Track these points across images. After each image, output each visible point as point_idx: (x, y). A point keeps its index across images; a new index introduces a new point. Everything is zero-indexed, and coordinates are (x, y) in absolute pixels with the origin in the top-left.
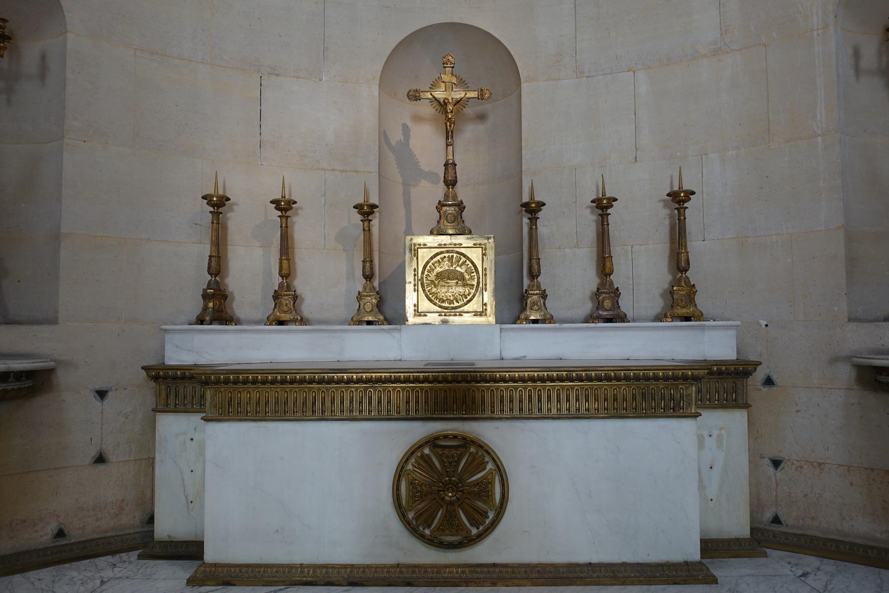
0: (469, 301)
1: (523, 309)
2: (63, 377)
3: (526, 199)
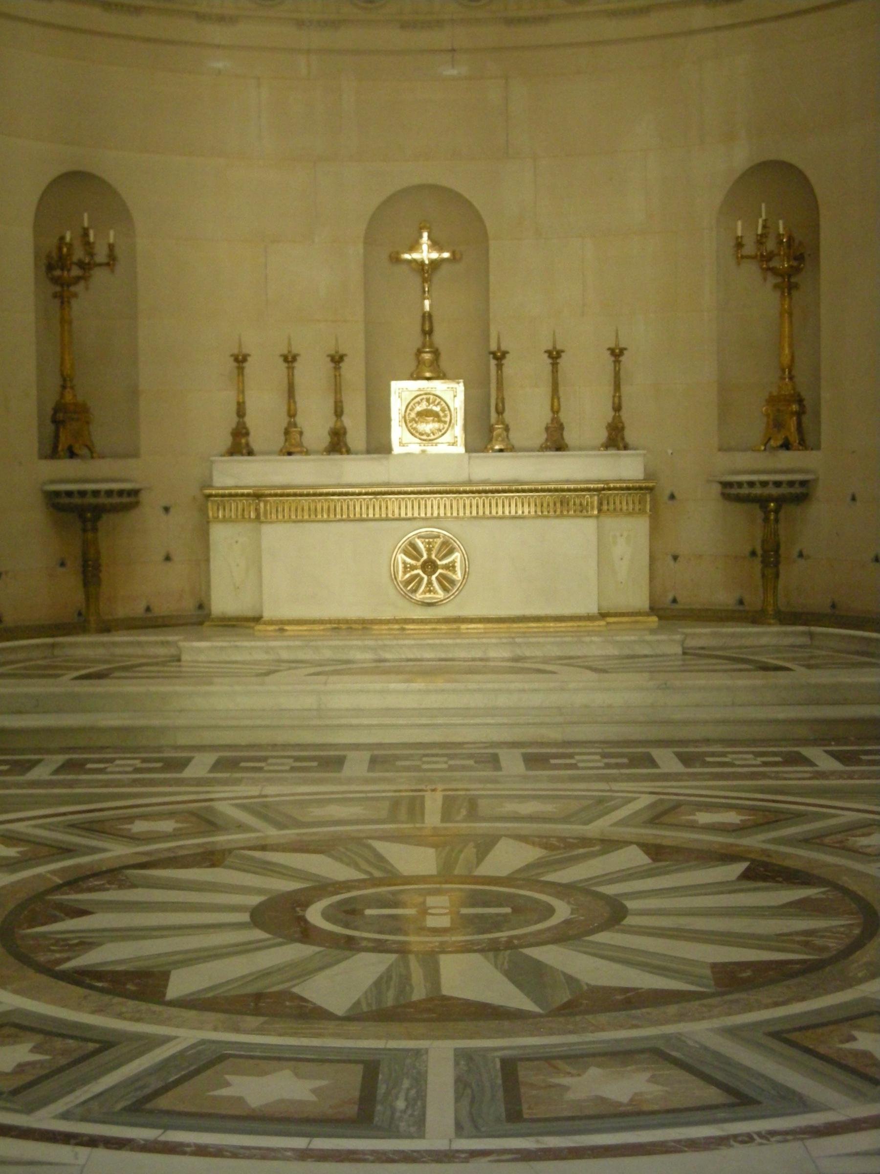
0: (443, 434)
1: (490, 440)
2: (144, 497)
3: (493, 347)
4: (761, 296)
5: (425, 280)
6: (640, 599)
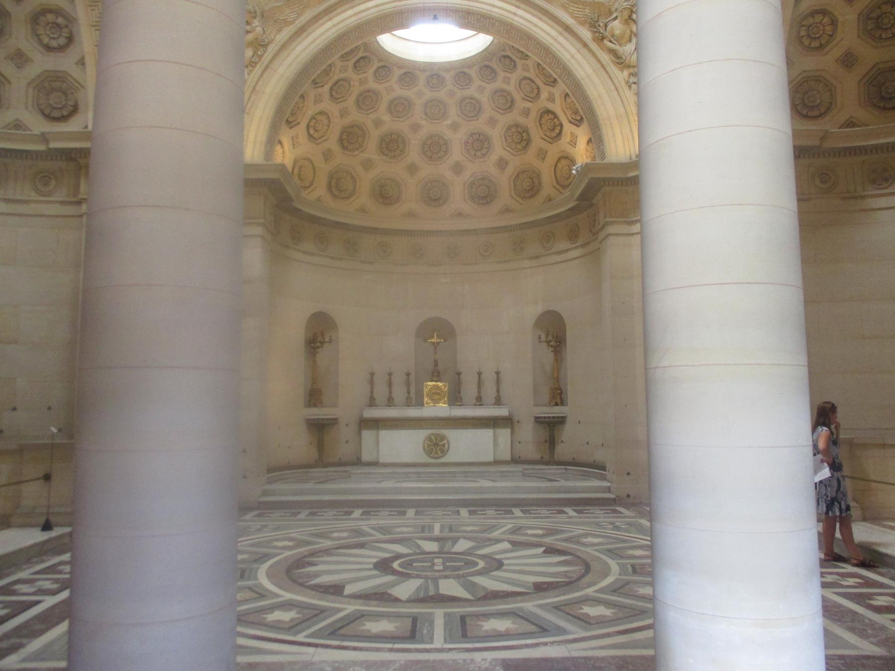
4: (548, 355)
5: (435, 349)
6: (507, 456)
